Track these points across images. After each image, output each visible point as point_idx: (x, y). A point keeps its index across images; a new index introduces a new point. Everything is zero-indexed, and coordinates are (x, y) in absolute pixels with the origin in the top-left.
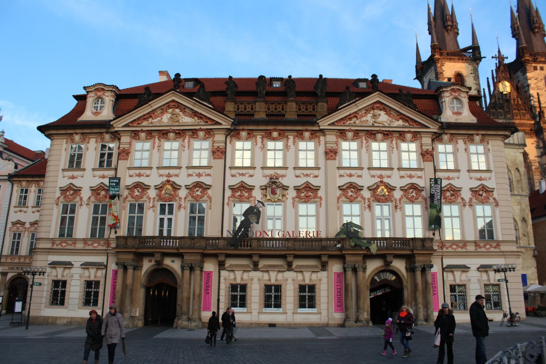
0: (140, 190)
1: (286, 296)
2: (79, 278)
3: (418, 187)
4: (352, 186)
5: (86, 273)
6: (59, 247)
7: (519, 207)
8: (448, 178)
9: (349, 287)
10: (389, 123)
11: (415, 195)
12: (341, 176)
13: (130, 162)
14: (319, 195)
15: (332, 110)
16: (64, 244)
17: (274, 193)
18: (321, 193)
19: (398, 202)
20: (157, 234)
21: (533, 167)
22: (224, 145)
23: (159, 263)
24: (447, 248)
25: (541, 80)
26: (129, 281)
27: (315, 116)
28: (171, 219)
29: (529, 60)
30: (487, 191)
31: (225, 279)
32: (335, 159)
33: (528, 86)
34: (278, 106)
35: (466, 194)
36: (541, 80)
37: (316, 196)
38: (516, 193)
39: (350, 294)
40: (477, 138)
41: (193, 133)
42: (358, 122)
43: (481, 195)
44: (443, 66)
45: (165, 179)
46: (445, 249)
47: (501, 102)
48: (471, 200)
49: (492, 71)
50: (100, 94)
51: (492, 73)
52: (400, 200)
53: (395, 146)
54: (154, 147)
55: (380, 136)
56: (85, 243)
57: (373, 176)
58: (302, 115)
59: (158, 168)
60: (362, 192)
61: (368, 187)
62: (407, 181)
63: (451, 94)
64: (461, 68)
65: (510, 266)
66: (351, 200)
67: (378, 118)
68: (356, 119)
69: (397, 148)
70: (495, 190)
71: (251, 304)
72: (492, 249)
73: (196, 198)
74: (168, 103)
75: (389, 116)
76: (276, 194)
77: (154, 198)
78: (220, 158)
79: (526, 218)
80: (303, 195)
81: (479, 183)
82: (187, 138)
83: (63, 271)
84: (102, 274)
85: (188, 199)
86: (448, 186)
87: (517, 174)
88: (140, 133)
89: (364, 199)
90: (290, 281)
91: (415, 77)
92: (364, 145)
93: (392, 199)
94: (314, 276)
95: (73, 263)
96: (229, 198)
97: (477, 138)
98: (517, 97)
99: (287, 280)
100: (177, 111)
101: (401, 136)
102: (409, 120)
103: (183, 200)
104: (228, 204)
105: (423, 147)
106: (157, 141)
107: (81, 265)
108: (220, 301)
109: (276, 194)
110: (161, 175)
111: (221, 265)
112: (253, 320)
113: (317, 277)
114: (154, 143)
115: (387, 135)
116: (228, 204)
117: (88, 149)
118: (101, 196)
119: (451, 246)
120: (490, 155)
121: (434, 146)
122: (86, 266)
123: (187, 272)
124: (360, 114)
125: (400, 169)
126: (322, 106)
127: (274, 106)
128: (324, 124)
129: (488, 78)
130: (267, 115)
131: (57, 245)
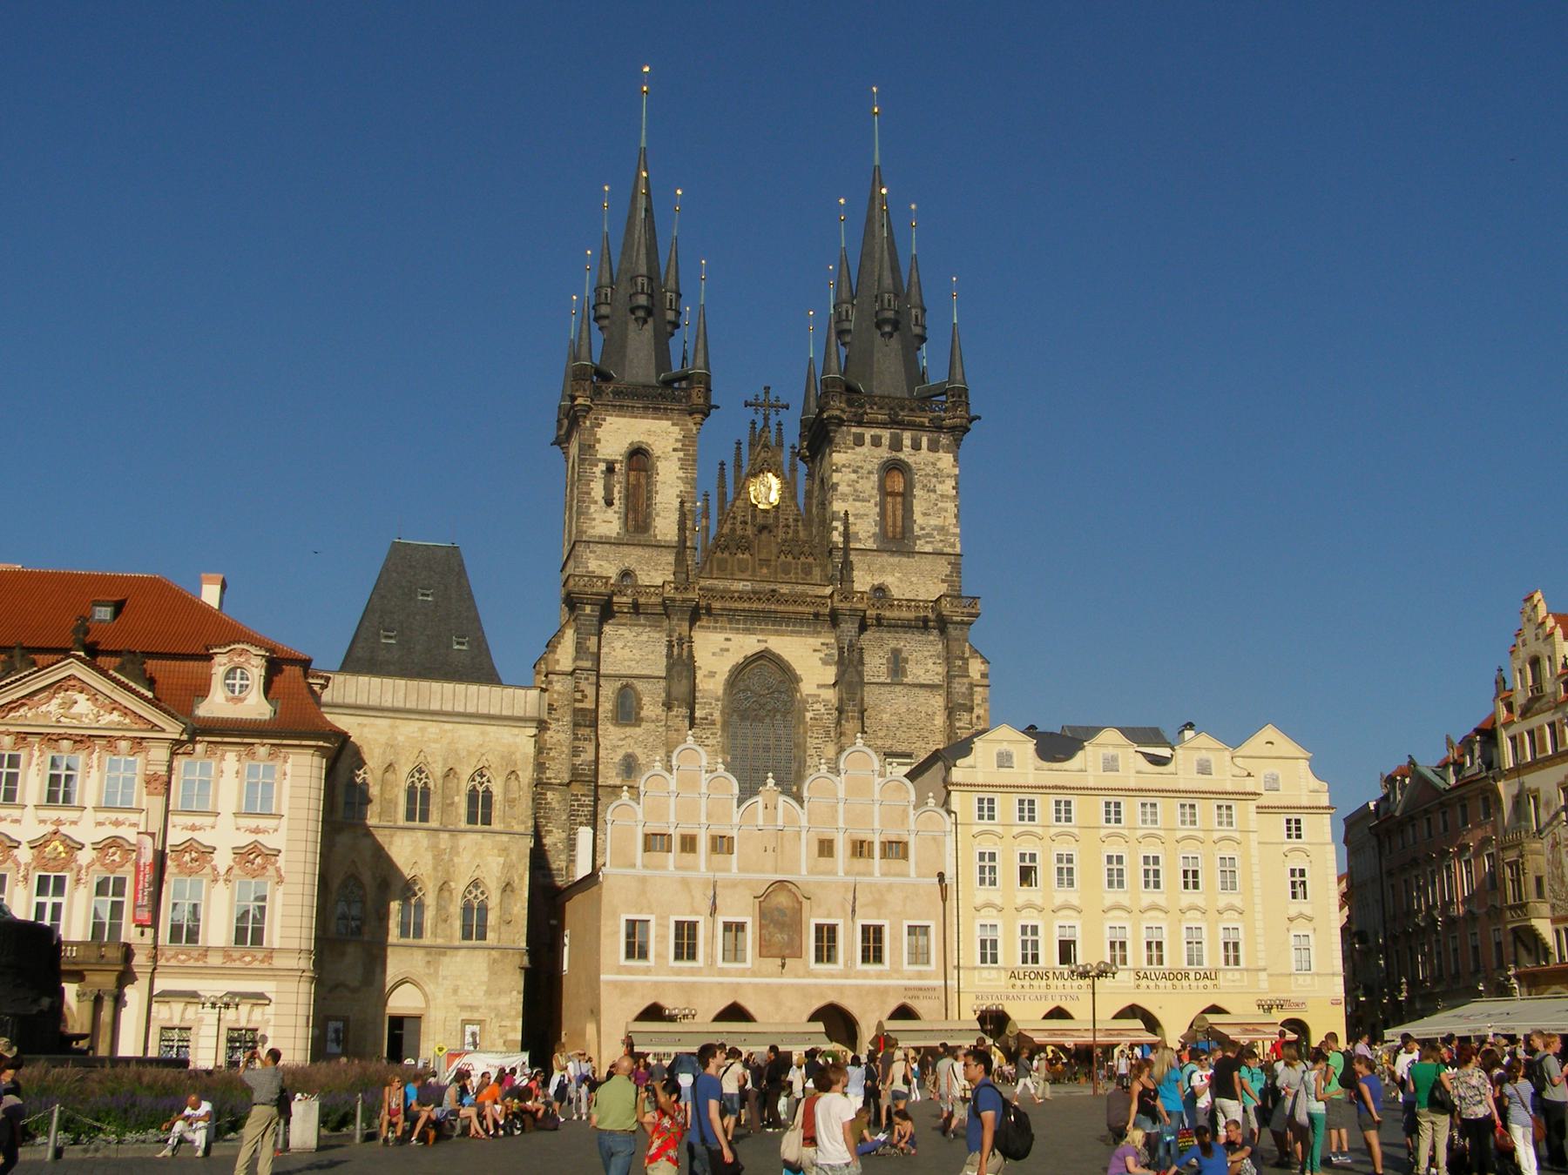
7: (501, 860)
8: (193, 828)
21: (809, 715)
25: (870, 472)
33: (834, 487)
35: (223, 859)
36: (870, 472)
40: (262, 751)
44: (599, 426)
46: (162, 962)
48: (230, 869)
49: (739, 443)
51: (739, 449)
57: (43, 822)
60: (16, 852)
62: (110, 831)
63: (231, 660)
72: (256, 964)
81: (251, 838)
87: (513, 784)
89: (18, 865)
92: (35, 761)
98: (796, 520)
119: (176, 956)
120: (287, 783)
125: (97, 809)
129: (722, 464)
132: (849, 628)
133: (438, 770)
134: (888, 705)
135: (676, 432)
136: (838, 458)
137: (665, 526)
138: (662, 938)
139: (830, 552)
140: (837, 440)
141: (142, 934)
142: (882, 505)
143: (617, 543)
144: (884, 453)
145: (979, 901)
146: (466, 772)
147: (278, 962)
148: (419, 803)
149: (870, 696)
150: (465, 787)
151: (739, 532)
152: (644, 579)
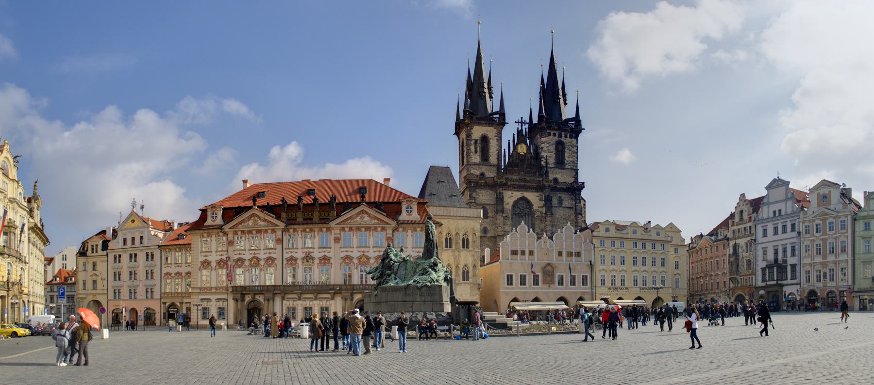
4: (347, 257)
15: (338, 216)
18: (332, 261)
55: (363, 229)
66: (348, 264)
91: (454, 132)
97: (419, 229)
101: (375, 229)
115: (368, 229)
132: (547, 191)
133: (454, 233)
134: (559, 213)
136: (543, 139)
137: (493, 159)
138: (517, 280)
142: (556, 154)
143: (479, 164)
144: (556, 138)
145: (601, 267)
146: (461, 234)
148: (449, 243)
149: (554, 210)
150: (461, 238)
152: (488, 175)
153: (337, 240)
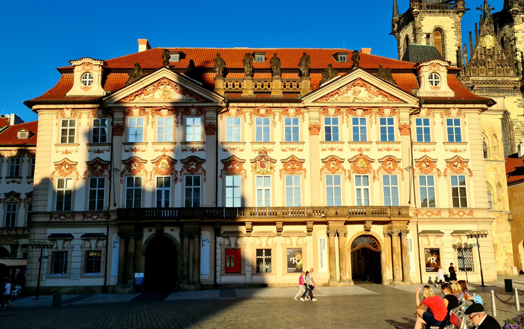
0: (137, 165)
1: (276, 259)
2: (80, 249)
3: (395, 159)
4: (333, 159)
5: (87, 244)
6: (58, 220)
7: (495, 173)
8: (425, 151)
9: (333, 251)
10: (369, 98)
11: (392, 167)
12: (324, 150)
13: (125, 137)
14: (304, 168)
16: (62, 217)
17: (262, 166)
18: (304, 166)
19: (376, 173)
20: (155, 206)
22: (215, 121)
23: (160, 232)
24: (422, 215)
26: (132, 249)
27: (299, 93)
28: (169, 191)
29: (517, 11)
30: (461, 162)
31: (220, 245)
32: (318, 134)
34: (265, 84)
35: (441, 165)
37: (301, 169)
38: (492, 159)
39: (333, 256)
41: (185, 110)
42: (339, 98)
43: (456, 166)
44: (422, 20)
45: (161, 154)
46: (420, 216)
47: (483, 58)
48: (446, 170)
49: (476, 24)
50: (88, 68)
51: (476, 26)
52: (378, 171)
53: (374, 121)
54: (148, 123)
56: (83, 216)
57: (353, 150)
58: (287, 92)
59: (153, 143)
60: (343, 164)
61: (348, 160)
62: (386, 153)
64: (442, 22)
65: (482, 233)
66: (333, 171)
67: (358, 95)
68: (337, 95)
69: (376, 122)
70: (470, 161)
71: (244, 267)
72: (465, 216)
73: (192, 171)
74: (159, 80)
75: (369, 92)
76: (264, 167)
77: (151, 172)
78: (213, 134)
79: (502, 183)
80: (289, 167)
81: (454, 154)
82: (180, 115)
83: (64, 243)
84: (103, 244)
85: (184, 172)
86: (424, 158)
87: (495, 140)
88: (133, 109)
89: (344, 170)
90: (279, 245)
92: (345, 121)
93: (371, 170)
94: (301, 240)
95: (73, 235)
96: (222, 171)
99: (276, 244)
100: (169, 87)
102: (388, 95)
103: (179, 174)
104: (221, 176)
105: (401, 122)
106: (150, 117)
107: (82, 236)
108: (217, 264)
109: (264, 167)
110: (156, 151)
111: (217, 233)
112: (247, 281)
113: (303, 241)
114: (148, 119)
116: (221, 176)
117: (80, 124)
118: (98, 170)
120: (467, 127)
121: (411, 120)
122: (87, 237)
123: (186, 240)
124: (342, 90)
126: (305, 84)
127: (260, 84)
128: (308, 101)
130: (255, 93)
131: (56, 218)
135: (452, 21)
139: (516, 64)
140: (515, 20)
141: (410, 202)
147: (476, 214)
151: (479, 58)
153: (314, 129)
